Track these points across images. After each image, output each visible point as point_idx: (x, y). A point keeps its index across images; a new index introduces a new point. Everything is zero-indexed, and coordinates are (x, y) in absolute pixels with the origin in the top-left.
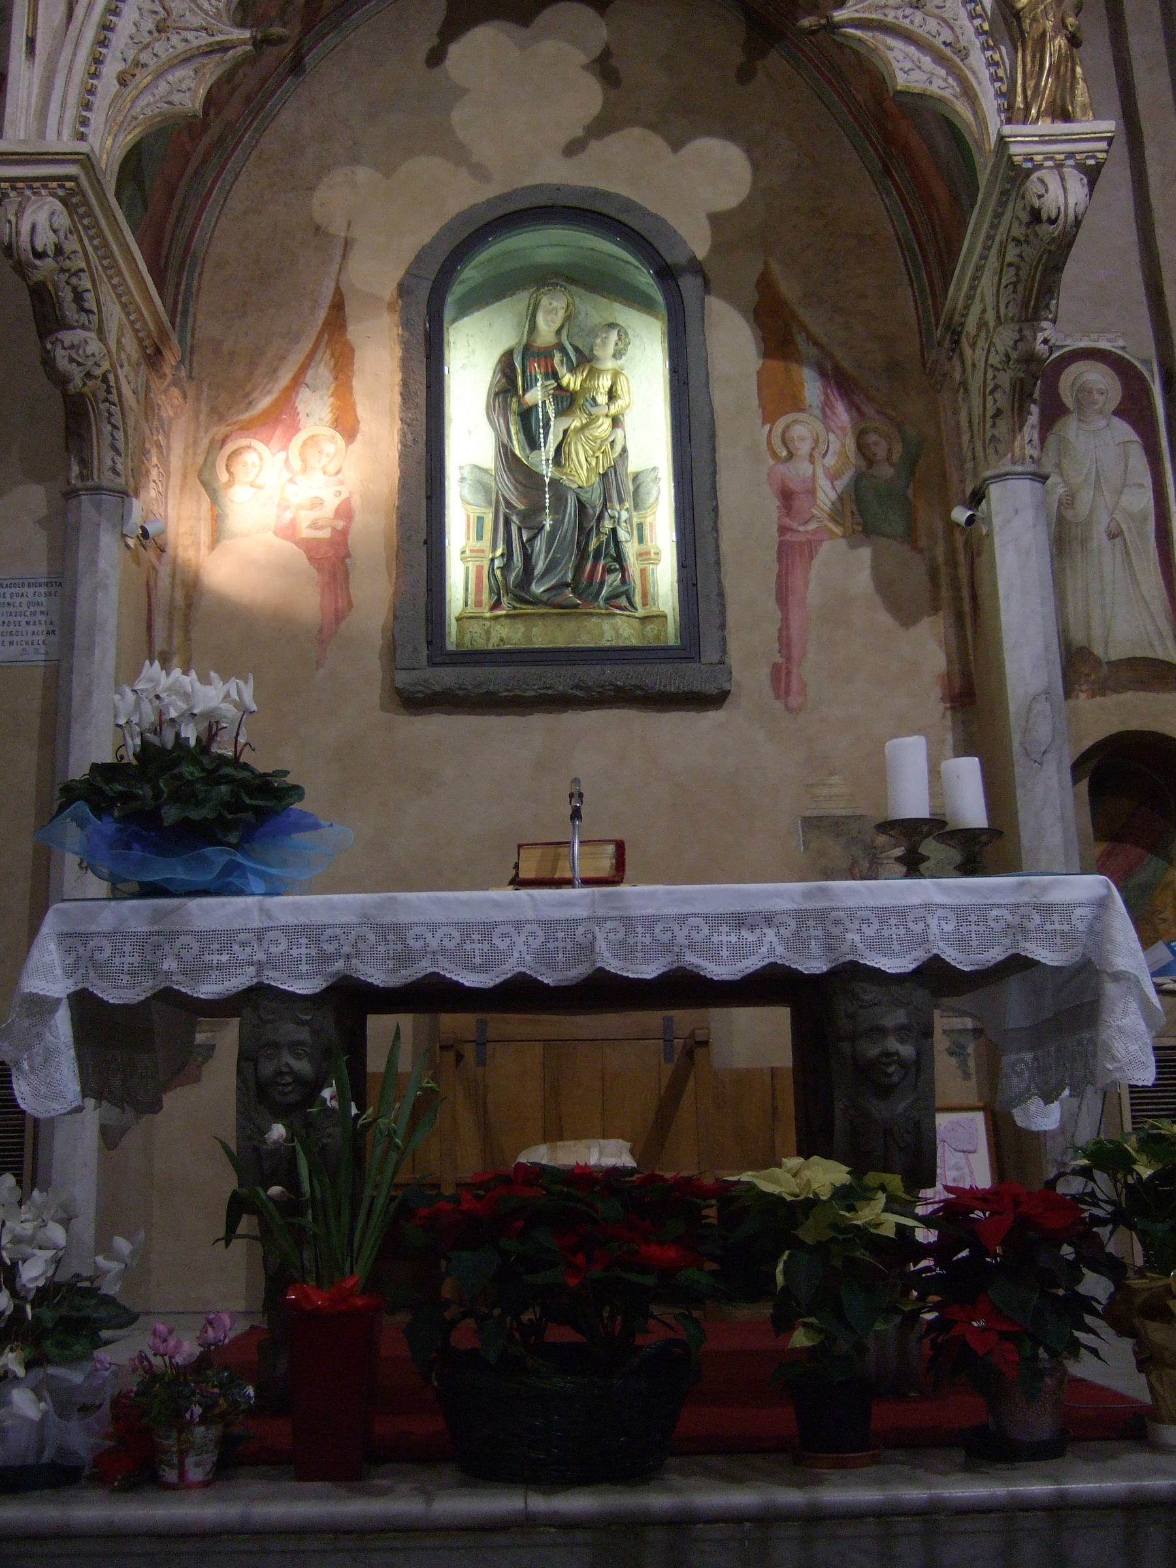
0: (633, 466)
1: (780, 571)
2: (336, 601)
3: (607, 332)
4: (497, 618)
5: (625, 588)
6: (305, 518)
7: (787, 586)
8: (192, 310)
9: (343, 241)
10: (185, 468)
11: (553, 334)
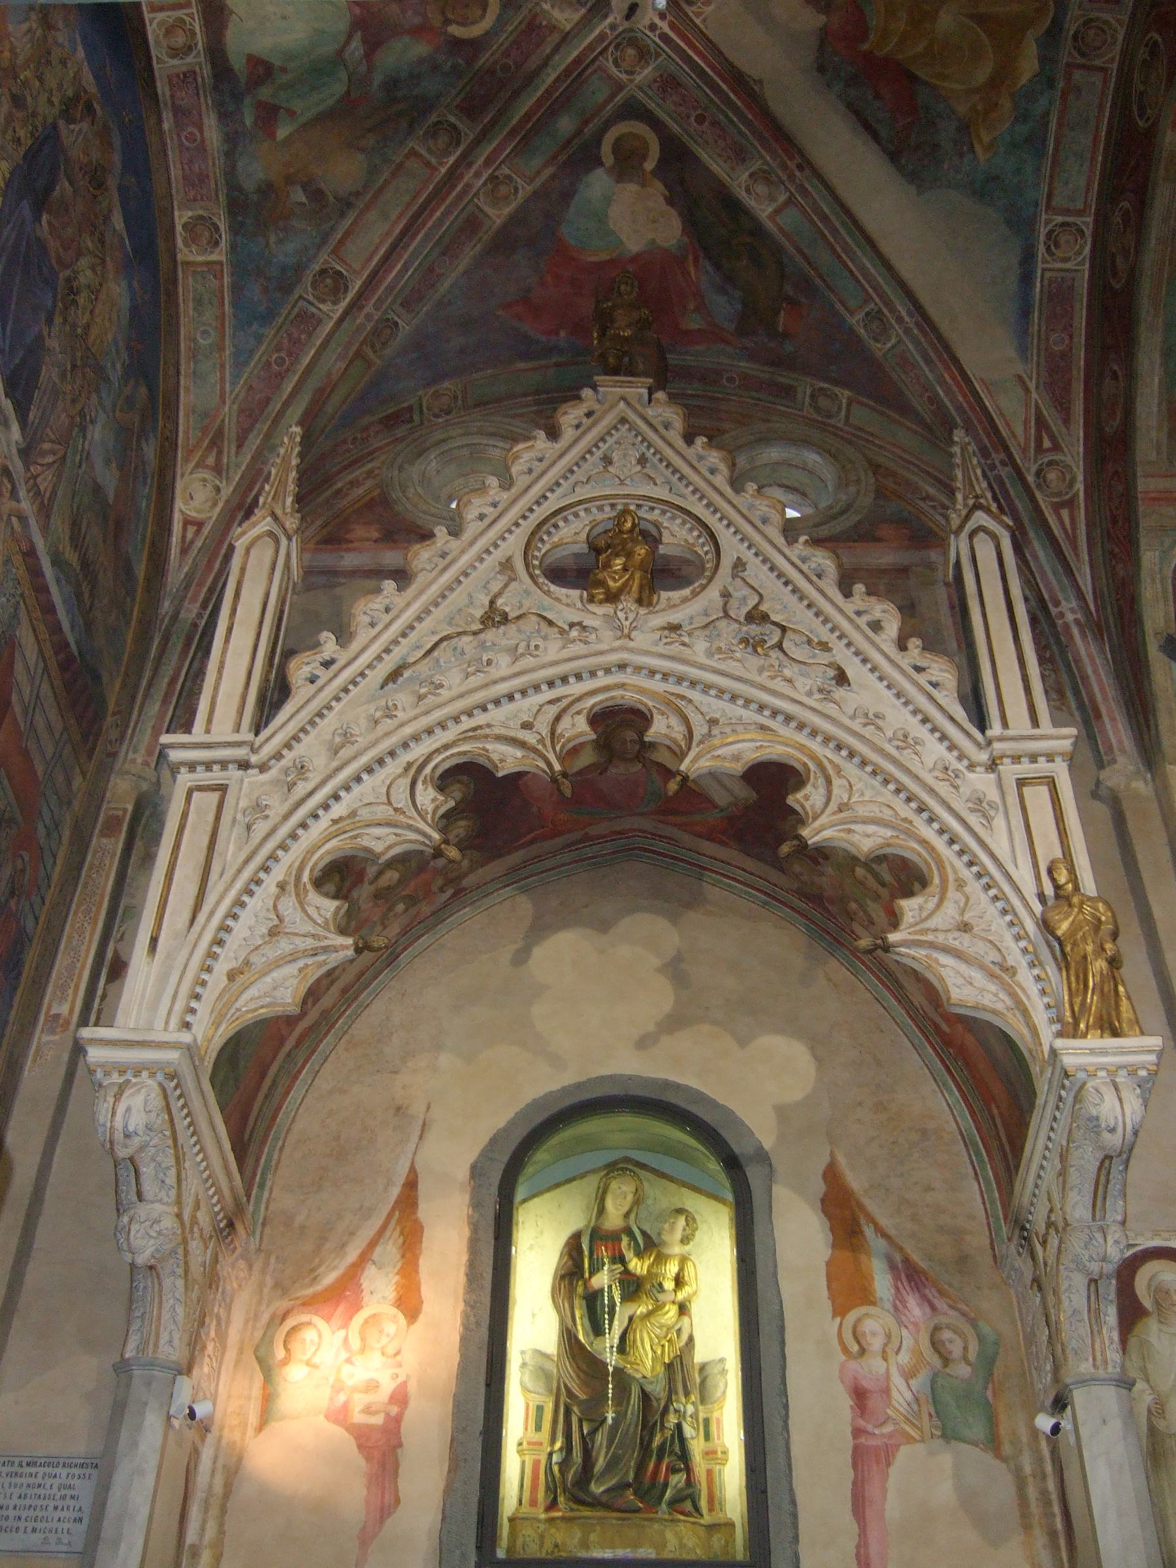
0: (700, 1356)
2: (383, 1496)
3: (676, 1218)
4: (551, 1520)
5: (690, 1491)
6: (359, 1401)
7: (863, 1496)
8: (269, 1183)
9: (420, 1122)
10: (242, 1342)
11: (622, 1218)
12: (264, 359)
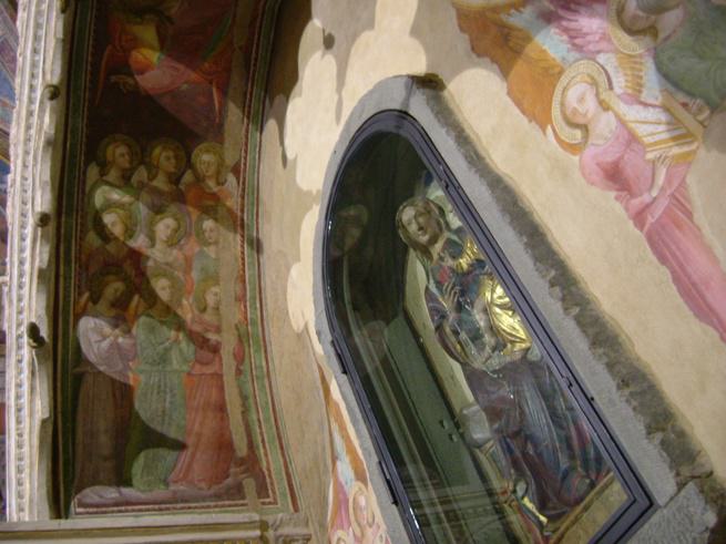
1: (673, 272)
7: (694, 284)
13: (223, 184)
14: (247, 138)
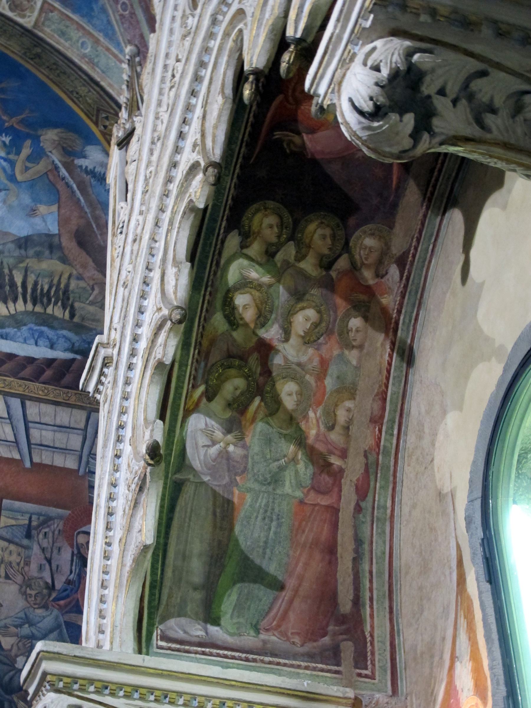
12: (118, 17)
13: (382, 278)
14: (423, 224)
